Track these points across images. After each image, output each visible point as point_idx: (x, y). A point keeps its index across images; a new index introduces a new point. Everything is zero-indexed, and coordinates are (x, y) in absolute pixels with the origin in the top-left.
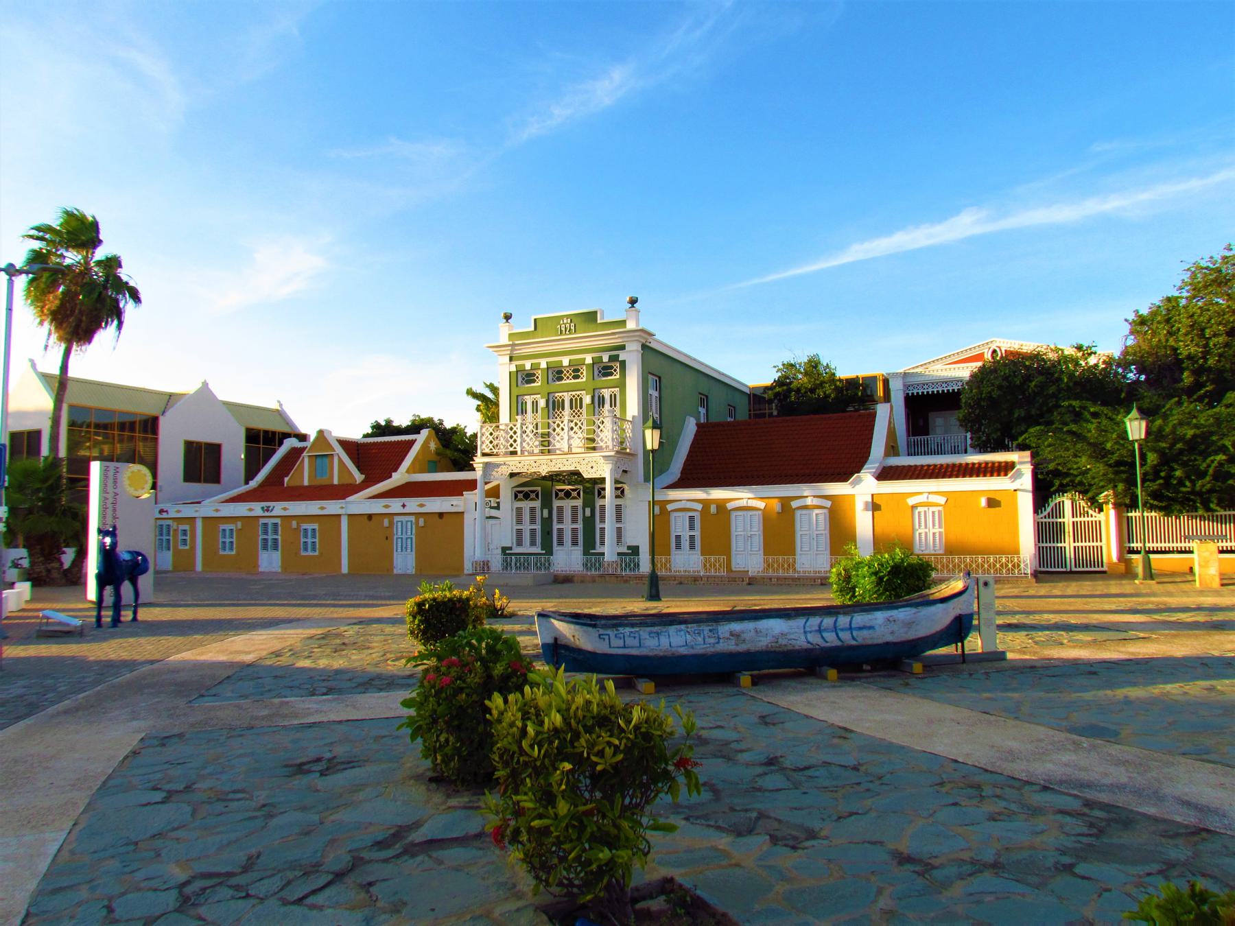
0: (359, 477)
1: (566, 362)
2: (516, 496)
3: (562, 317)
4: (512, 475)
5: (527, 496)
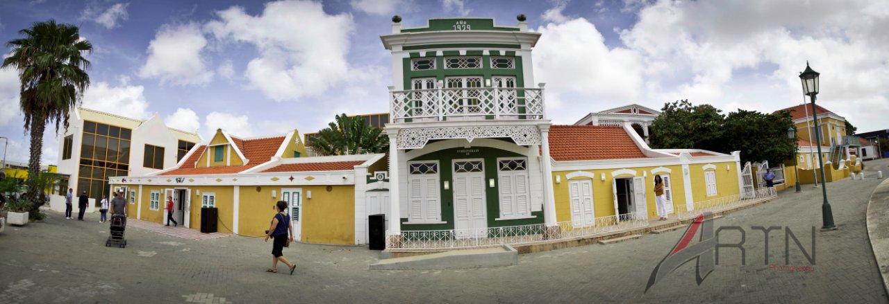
0: (245, 161)
1: (463, 52)
2: (412, 169)
3: (459, 20)
4: (407, 151)
5: (423, 169)
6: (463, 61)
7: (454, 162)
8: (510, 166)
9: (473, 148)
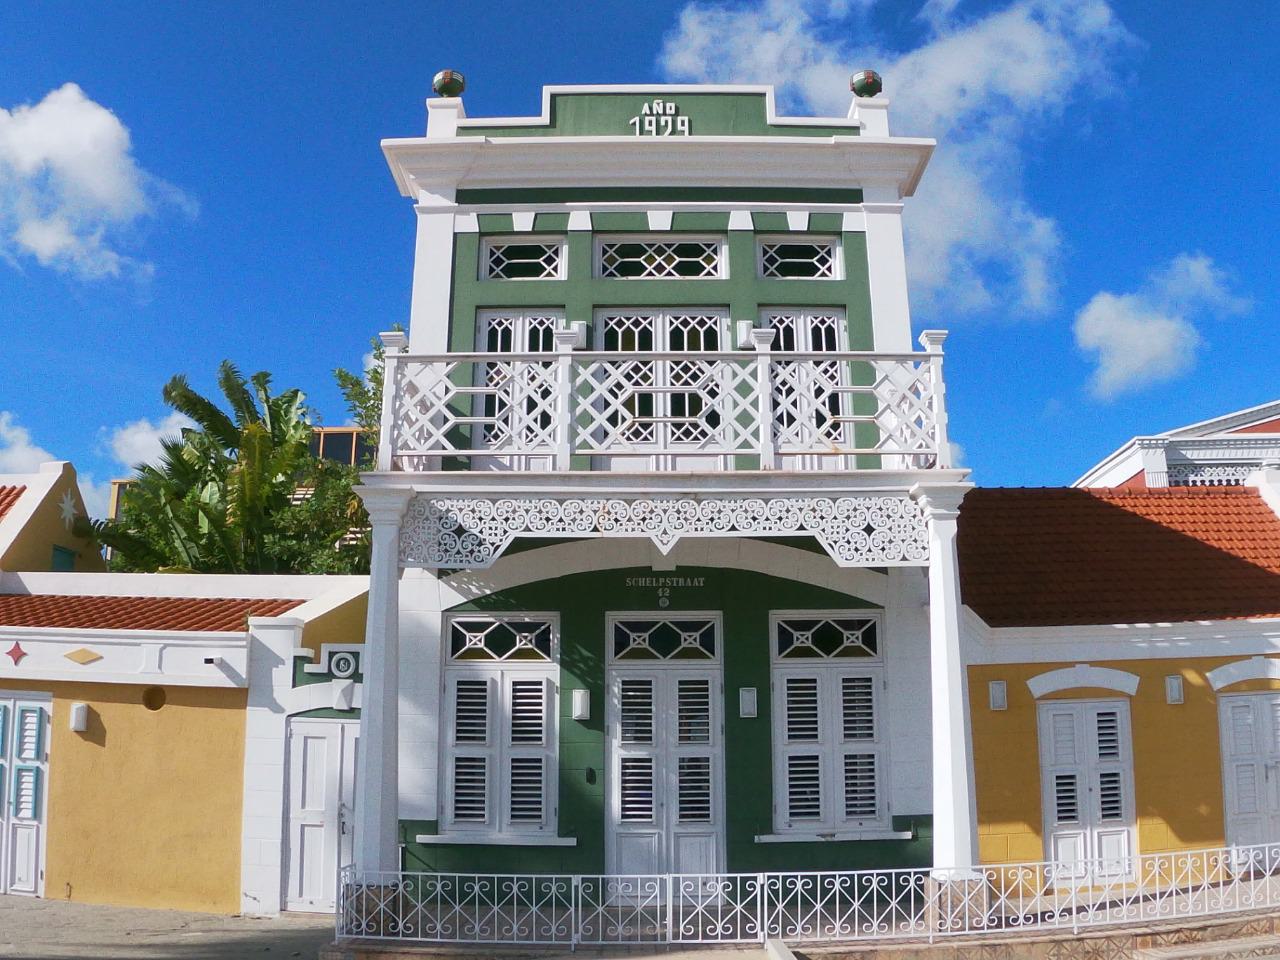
2: (458, 640)
6: (660, 251)
7: (613, 618)
8: (816, 639)
9: (682, 571)
